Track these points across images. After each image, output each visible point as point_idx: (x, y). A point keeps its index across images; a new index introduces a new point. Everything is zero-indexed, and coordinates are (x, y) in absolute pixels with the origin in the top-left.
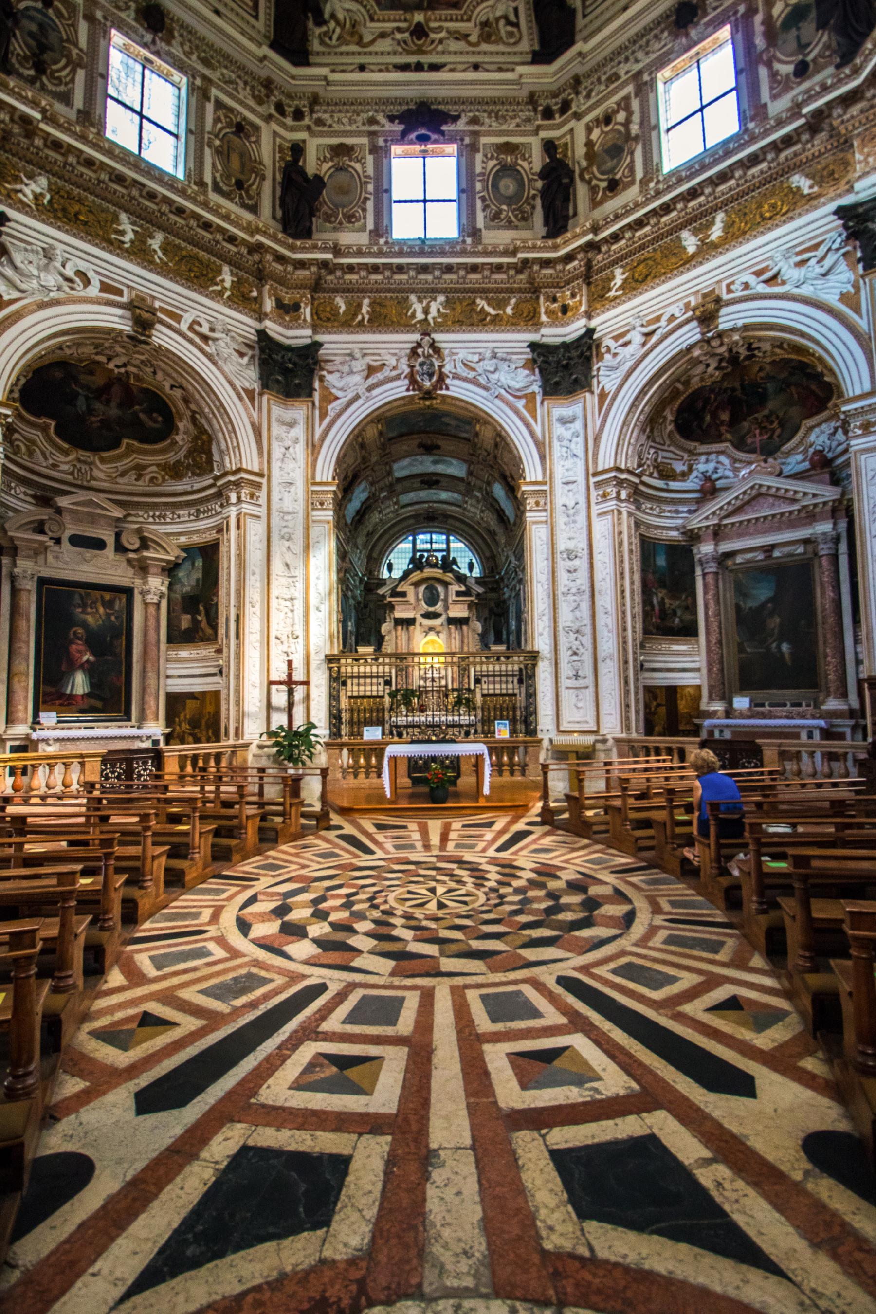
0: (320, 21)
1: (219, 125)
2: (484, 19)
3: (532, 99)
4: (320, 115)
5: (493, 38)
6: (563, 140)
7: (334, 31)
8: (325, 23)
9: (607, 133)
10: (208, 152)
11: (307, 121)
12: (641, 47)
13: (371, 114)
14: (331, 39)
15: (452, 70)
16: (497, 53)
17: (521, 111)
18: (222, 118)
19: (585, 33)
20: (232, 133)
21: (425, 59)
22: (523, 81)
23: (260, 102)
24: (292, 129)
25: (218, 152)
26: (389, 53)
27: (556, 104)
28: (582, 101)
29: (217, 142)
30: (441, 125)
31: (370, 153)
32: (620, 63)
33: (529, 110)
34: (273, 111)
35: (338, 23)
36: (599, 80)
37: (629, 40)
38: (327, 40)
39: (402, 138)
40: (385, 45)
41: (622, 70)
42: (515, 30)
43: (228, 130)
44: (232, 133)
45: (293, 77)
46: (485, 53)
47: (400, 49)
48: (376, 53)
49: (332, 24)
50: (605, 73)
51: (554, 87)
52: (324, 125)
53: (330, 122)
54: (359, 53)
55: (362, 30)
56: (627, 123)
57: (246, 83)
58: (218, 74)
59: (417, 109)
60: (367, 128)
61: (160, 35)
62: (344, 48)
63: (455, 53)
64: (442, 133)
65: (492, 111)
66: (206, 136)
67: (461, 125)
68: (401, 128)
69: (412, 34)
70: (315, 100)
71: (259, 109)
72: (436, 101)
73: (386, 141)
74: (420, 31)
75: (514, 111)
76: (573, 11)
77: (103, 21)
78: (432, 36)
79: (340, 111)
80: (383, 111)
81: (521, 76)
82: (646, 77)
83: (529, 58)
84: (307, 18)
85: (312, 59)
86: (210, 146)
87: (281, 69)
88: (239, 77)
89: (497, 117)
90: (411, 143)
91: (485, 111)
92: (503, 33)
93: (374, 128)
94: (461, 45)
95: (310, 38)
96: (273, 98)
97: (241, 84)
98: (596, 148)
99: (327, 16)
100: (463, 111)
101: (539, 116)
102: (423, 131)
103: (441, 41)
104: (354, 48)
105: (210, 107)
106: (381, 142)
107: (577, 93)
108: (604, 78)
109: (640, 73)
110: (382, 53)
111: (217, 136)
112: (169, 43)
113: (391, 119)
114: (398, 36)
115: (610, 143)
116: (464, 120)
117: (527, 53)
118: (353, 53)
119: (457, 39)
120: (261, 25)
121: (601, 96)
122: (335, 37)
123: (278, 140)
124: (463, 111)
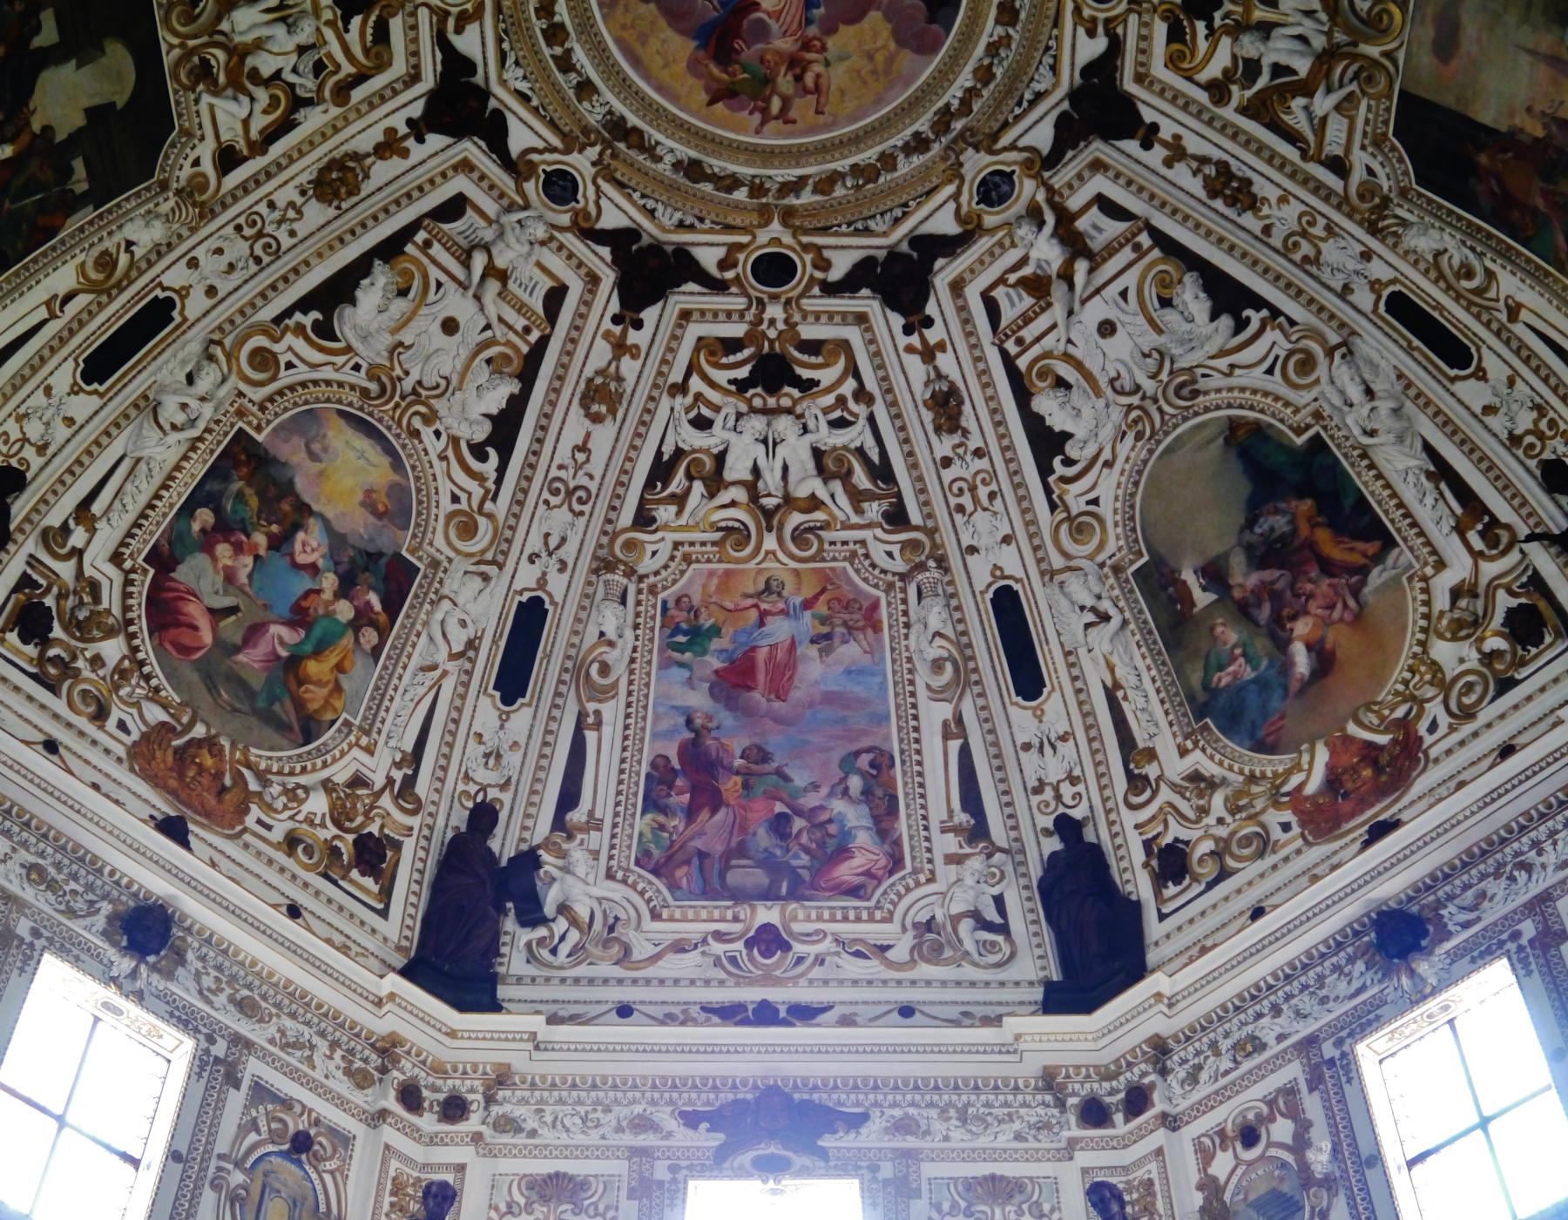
0: (532, 915)
1: (252, 1137)
2: (923, 917)
3: (1050, 1081)
4: (507, 1108)
5: (948, 953)
6: (1139, 1174)
7: (562, 938)
8: (544, 921)
9: (1250, 1164)
10: (208, 1197)
11: (473, 1123)
12: (1305, 987)
13: (638, 1109)
14: (554, 951)
15: (847, 1021)
16: (958, 984)
17: (1025, 1105)
18: (262, 1123)
19: (1167, 949)
20: (280, 1154)
21: (780, 996)
22: (1022, 1046)
23: (362, 1080)
24: (434, 1141)
25: (234, 1199)
26: (693, 982)
27: (1113, 1092)
28: (1178, 1090)
29: (238, 1178)
30: (819, 1136)
31: (632, 1194)
32: (1259, 1016)
33: (1045, 1104)
34: (392, 1103)
35: (574, 922)
36: (1214, 1045)
37: (1274, 975)
38: (545, 953)
39: (717, 1164)
40: (686, 964)
41: (1268, 1029)
42: (1000, 939)
43: (271, 1148)
44: (280, 1154)
45: (452, 1034)
46: (929, 983)
47: (723, 975)
48: (662, 982)
49: (561, 925)
50: (1227, 1035)
51: (1106, 1058)
52: (519, 1130)
53: (531, 1124)
54: (620, 981)
55: (631, 936)
56: (1300, 1144)
57: (334, 1045)
58: (272, 1030)
59: (758, 1101)
60: (628, 1139)
61: (151, 959)
62: (583, 970)
63: (855, 982)
64: (823, 1154)
65: (950, 1104)
66: (214, 1163)
67: (871, 1136)
68: (718, 1139)
69: (749, 944)
70: (502, 1078)
71: (359, 1098)
72: (805, 1083)
73: (674, 1169)
74: (769, 941)
75: (1006, 1104)
76: (1136, 907)
77: (28, 939)
78: (798, 948)
79: (561, 1101)
80: (671, 1102)
81: (1017, 1037)
82: (1329, 1050)
83: (1038, 994)
84: (504, 912)
85: (503, 992)
86: (216, 1187)
87: (425, 1018)
88: (322, 1034)
89: (963, 1119)
90: (740, 1174)
91: (931, 1105)
92: (969, 945)
93: (647, 1140)
94: (871, 968)
95: (504, 950)
96: (395, 1073)
97: (323, 1046)
98: (1227, 1197)
99: (549, 909)
100: (876, 1104)
101: (1073, 1119)
102: (772, 1149)
103: (820, 960)
104: (606, 969)
105: (236, 1100)
106: (661, 1171)
107: (1164, 1072)
108: (1225, 1045)
109: (1312, 1041)
110: (676, 982)
111: (238, 1164)
112: (169, 975)
113: (691, 1120)
114: (717, 948)
115: (1262, 1189)
116: (876, 1124)
117: (1031, 983)
118: (606, 981)
119: (858, 954)
120: (391, 928)
121: (1222, 1082)
122: (564, 949)
123: (394, 1164)
124: (876, 1104)
